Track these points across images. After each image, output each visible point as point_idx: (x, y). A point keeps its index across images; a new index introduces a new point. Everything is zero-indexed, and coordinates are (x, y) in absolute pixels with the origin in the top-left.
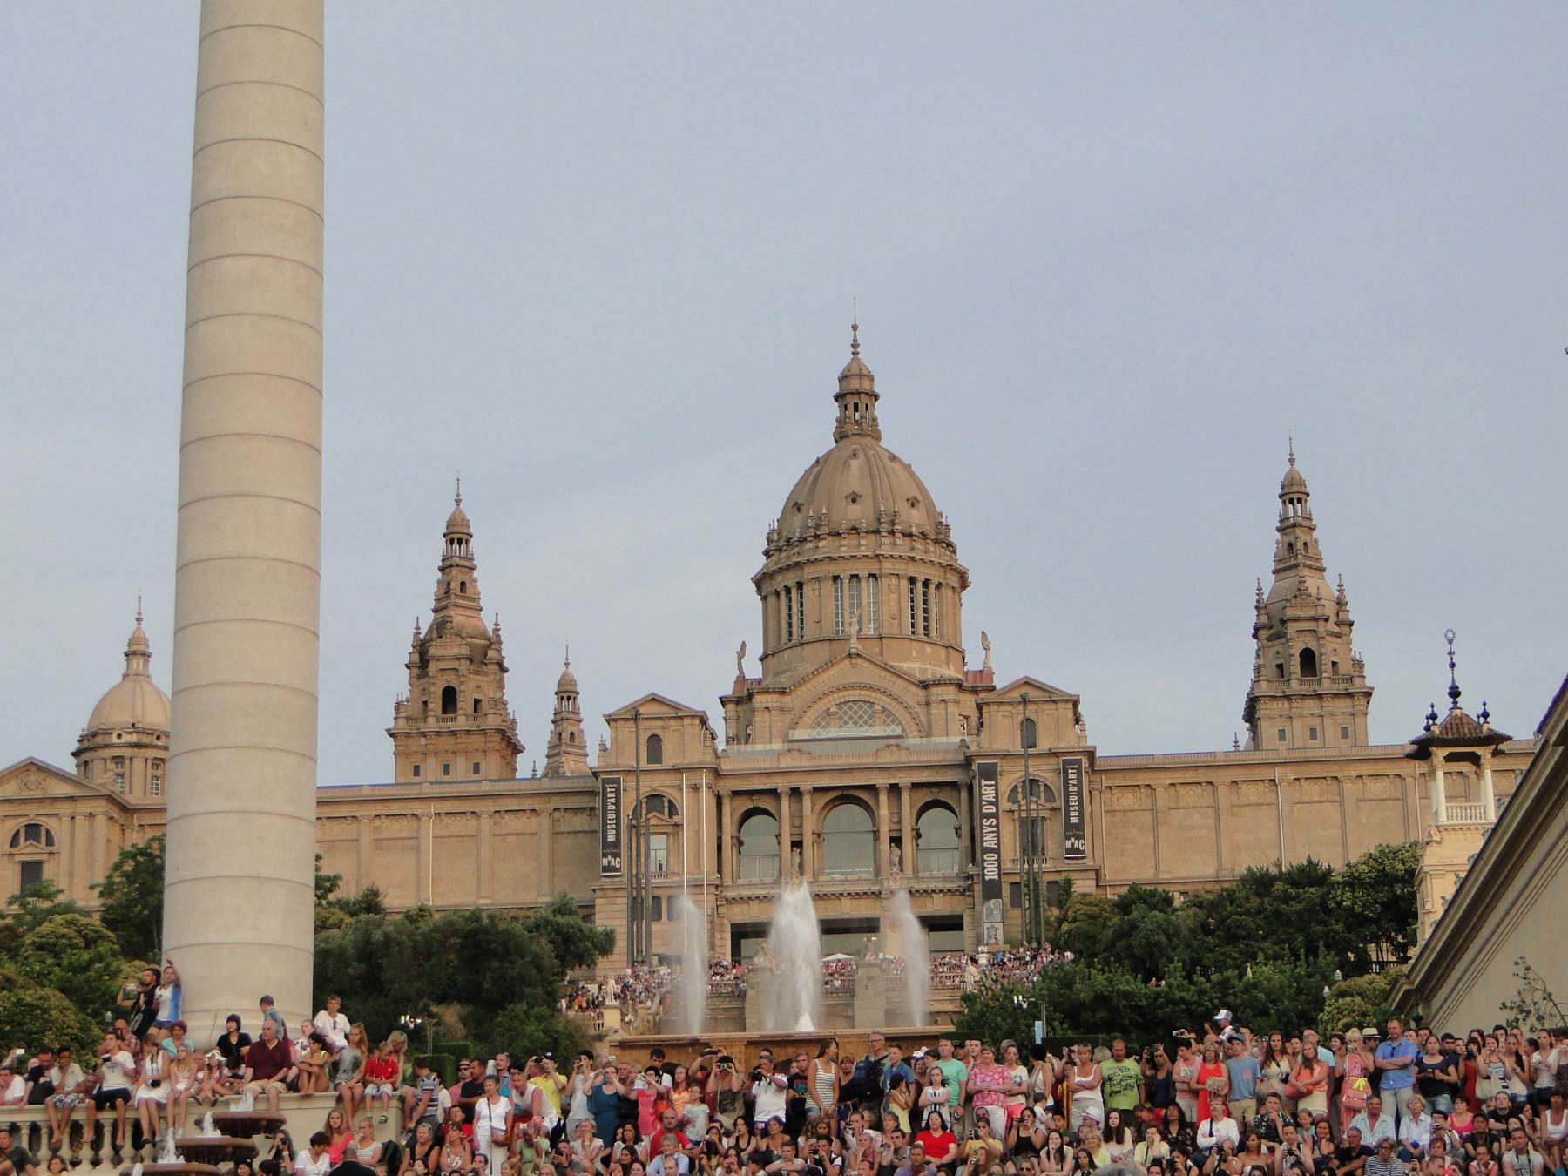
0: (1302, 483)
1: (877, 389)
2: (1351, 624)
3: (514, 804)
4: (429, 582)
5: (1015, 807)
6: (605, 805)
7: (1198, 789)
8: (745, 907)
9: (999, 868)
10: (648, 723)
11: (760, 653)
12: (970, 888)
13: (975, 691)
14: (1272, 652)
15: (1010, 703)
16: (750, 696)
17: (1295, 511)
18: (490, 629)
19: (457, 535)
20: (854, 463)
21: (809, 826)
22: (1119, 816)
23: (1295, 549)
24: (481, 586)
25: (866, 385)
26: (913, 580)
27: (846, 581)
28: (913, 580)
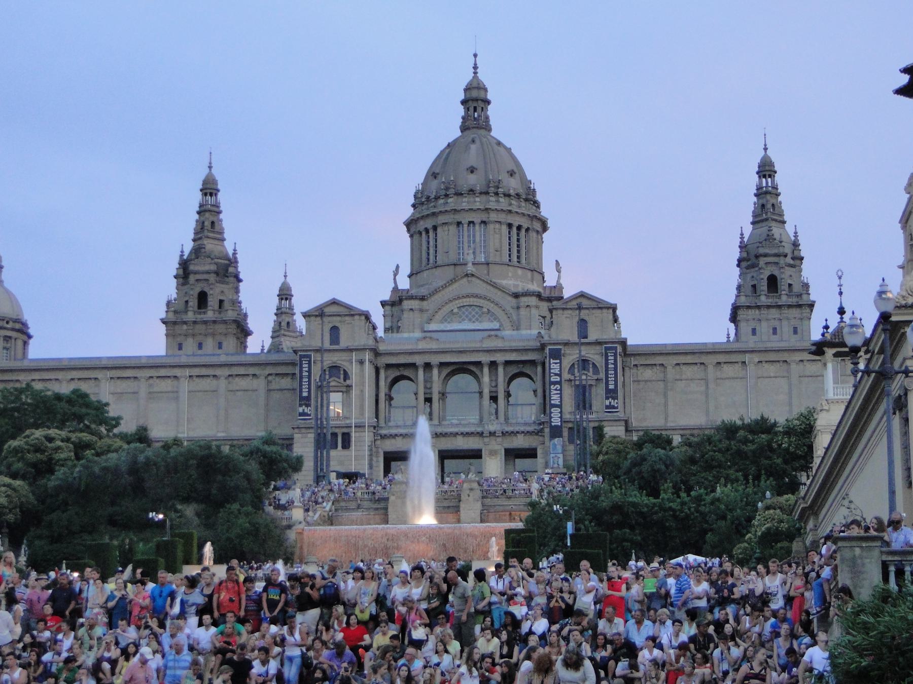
0: (771, 164)
1: (489, 97)
2: (802, 259)
3: (242, 371)
4: (191, 220)
5: (572, 378)
6: (301, 371)
7: (695, 368)
8: (393, 441)
9: (561, 417)
10: (330, 318)
11: (408, 272)
12: (542, 431)
13: (549, 300)
14: (749, 276)
15: (571, 309)
16: (401, 301)
17: (767, 183)
18: (230, 252)
19: (209, 189)
20: (473, 147)
21: (436, 388)
22: (642, 384)
23: (767, 206)
24: (225, 224)
25: (482, 95)
26: (510, 226)
27: (465, 226)
28: (510, 226)
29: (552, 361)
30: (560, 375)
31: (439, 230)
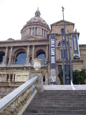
1: (40, 12)
5: (60, 47)
26: (43, 29)
29: (52, 40)
30: (55, 44)
31: (26, 30)
